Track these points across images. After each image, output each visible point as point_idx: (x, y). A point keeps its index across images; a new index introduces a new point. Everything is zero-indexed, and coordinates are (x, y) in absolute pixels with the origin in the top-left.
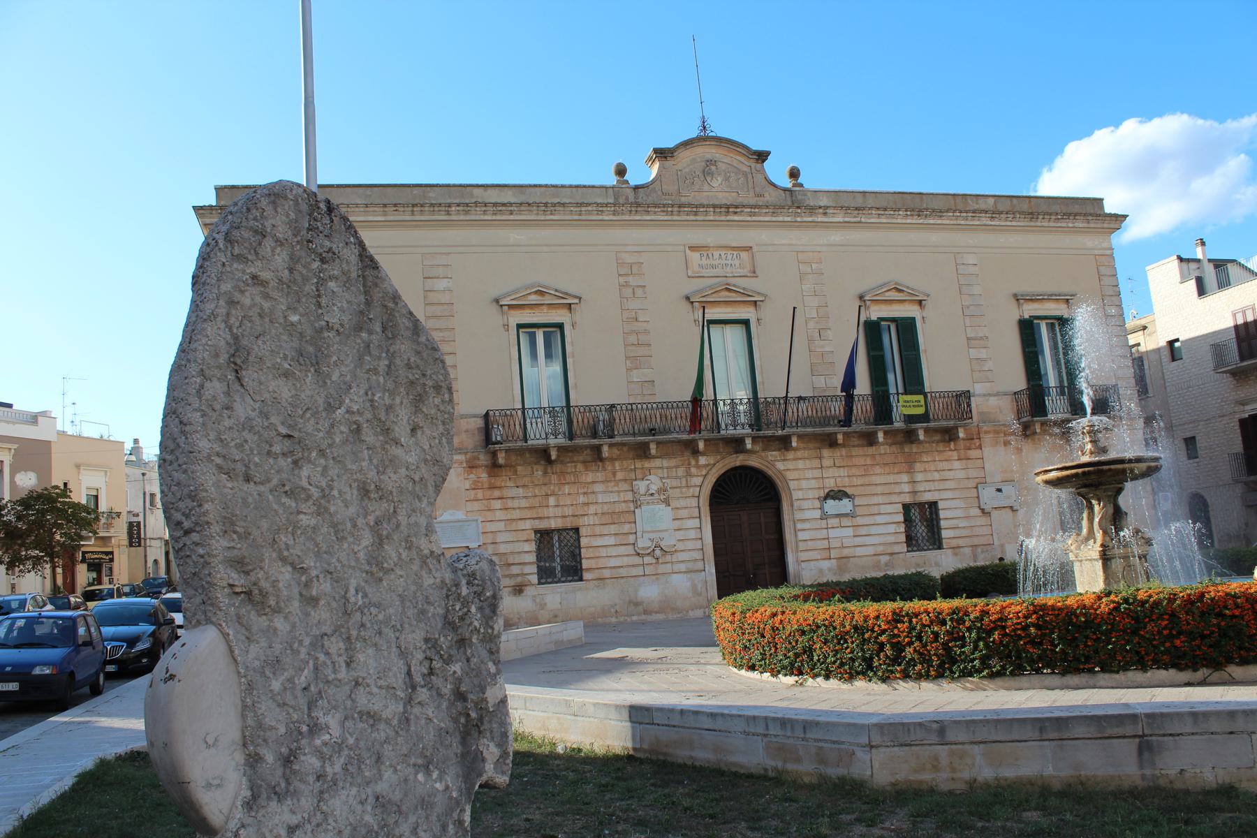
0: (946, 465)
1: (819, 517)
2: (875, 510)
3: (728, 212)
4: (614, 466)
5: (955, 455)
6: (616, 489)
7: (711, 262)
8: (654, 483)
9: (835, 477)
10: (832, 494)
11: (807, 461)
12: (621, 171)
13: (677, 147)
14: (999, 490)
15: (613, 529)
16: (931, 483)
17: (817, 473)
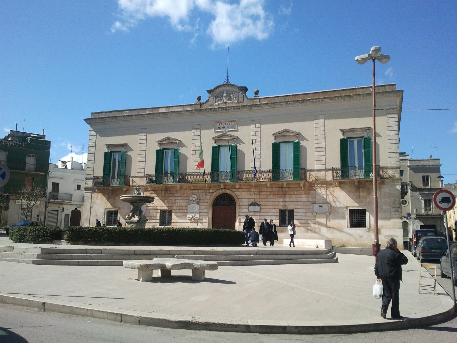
0: (299, 196)
1: (247, 211)
2: (268, 210)
3: (226, 109)
4: (184, 191)
5: (303, 192)
6: (184, 199)
7: (223, 126)
8: (194, 197)
9: (254, 198)
10: (253, 204)
11: (246, 192)
12: (199, 98)
13: (214, 89)
14: (321, 206)
15: (182, 211)
16: (292, 202)
17: (248, 197)
